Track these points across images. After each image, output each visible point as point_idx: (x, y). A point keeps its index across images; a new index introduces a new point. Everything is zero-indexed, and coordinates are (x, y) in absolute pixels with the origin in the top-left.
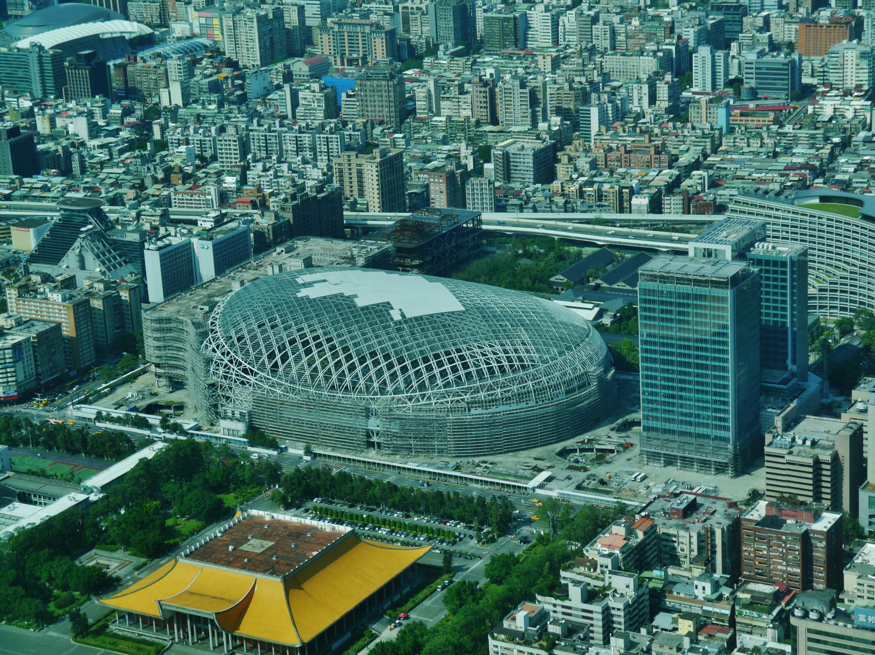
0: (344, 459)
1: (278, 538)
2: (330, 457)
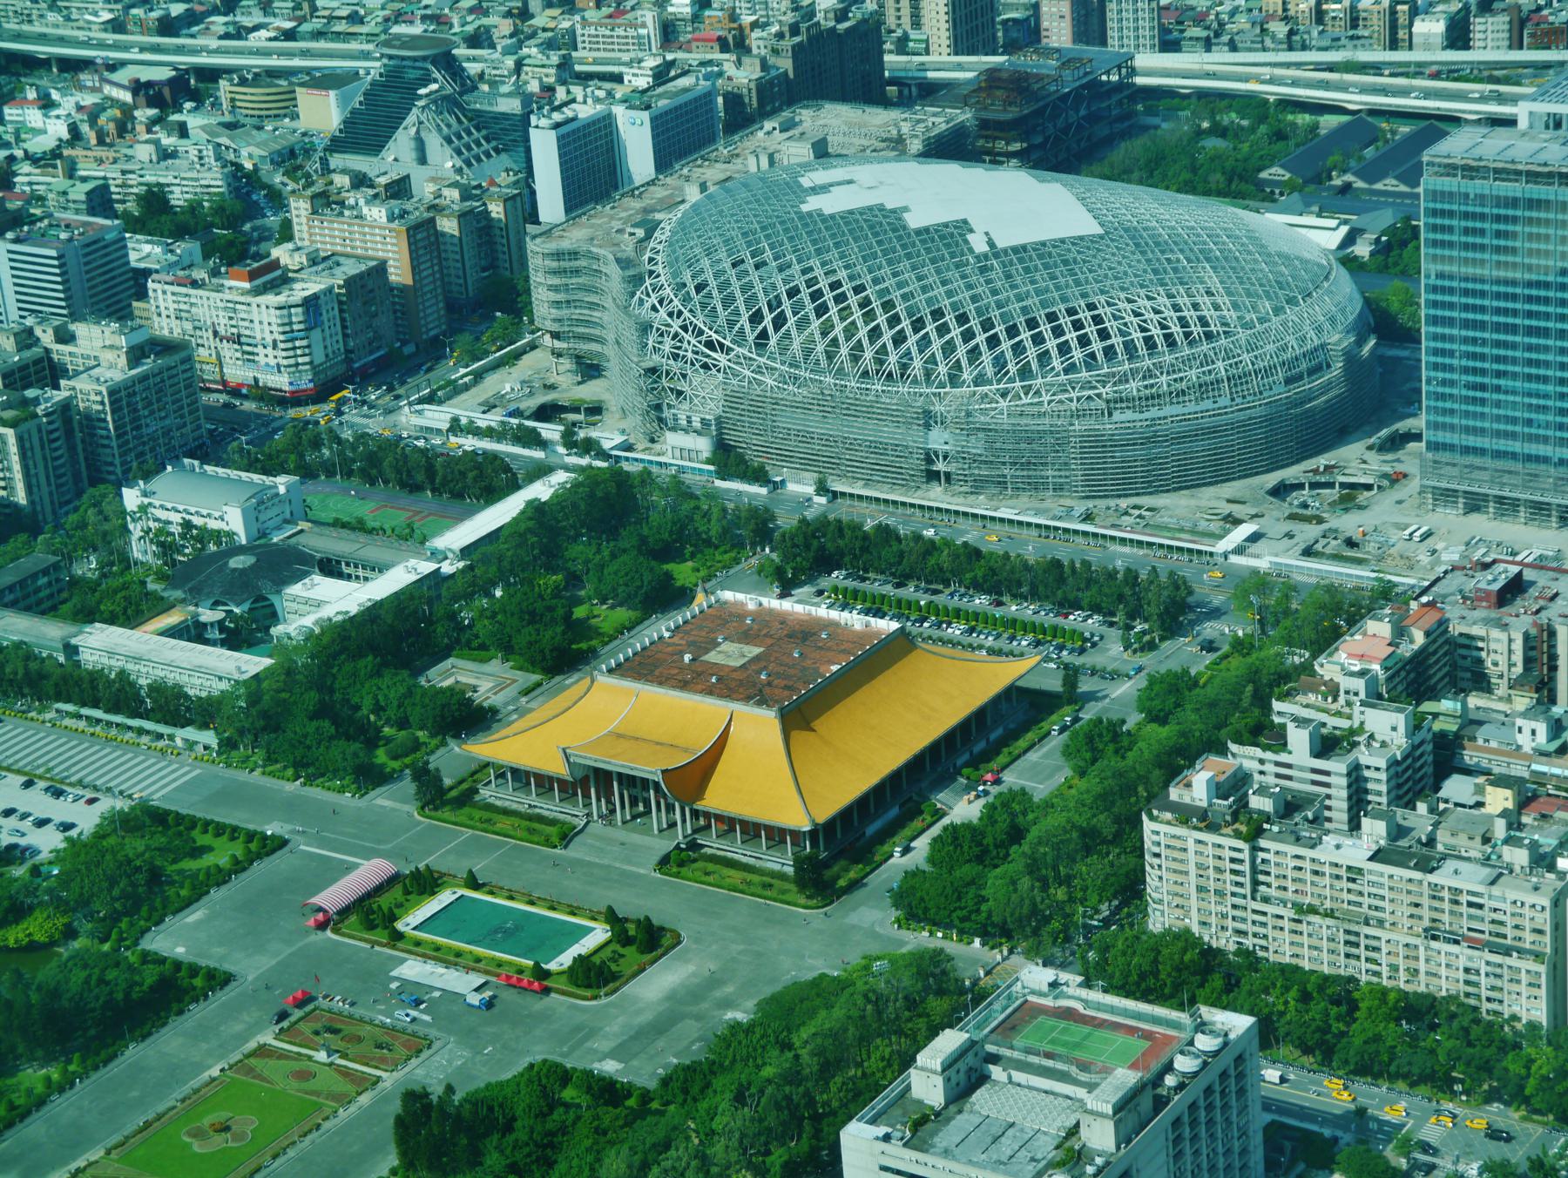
0: (886, 501)
1: (770, 641)
2: (860, 497)
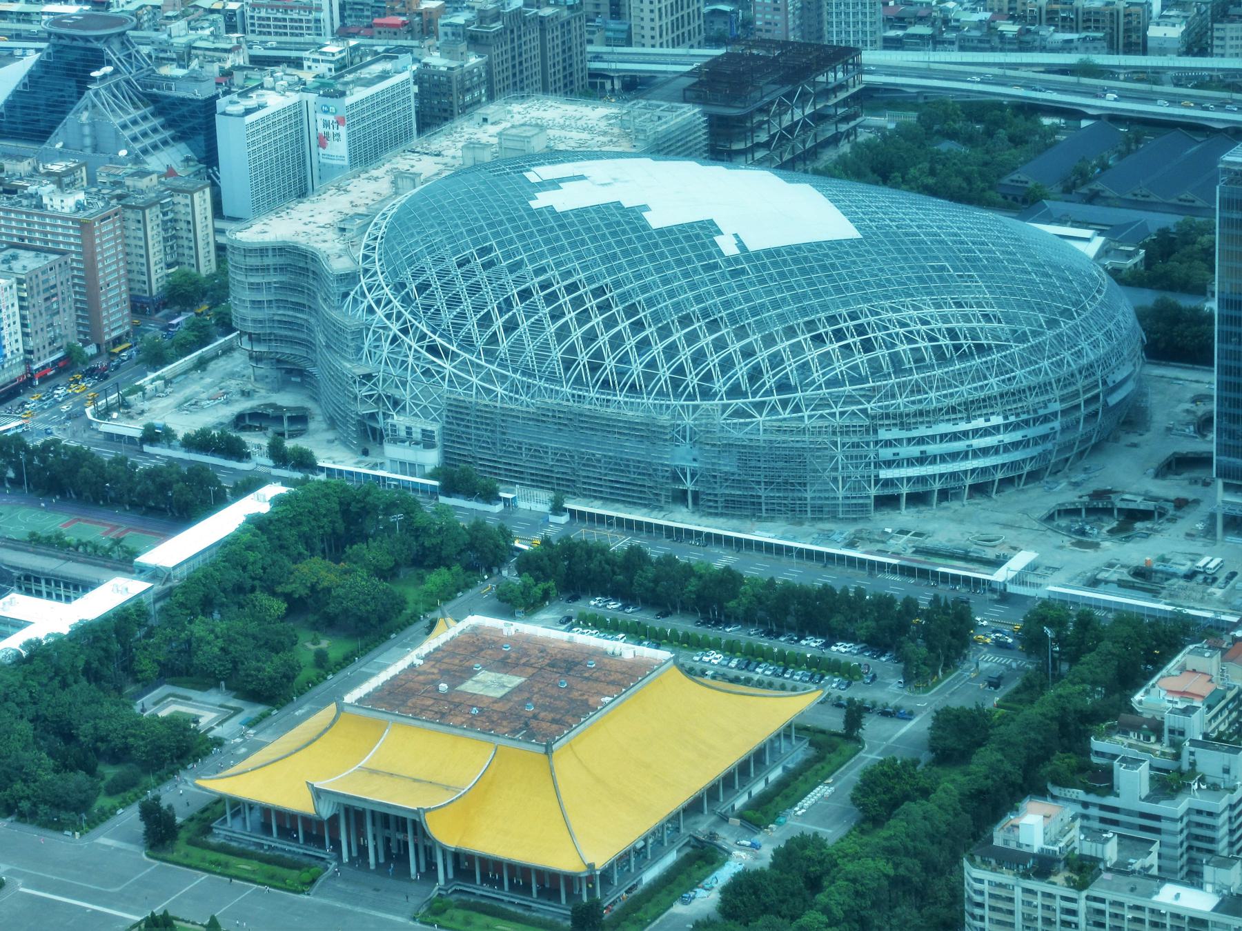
1: (530, 671)
